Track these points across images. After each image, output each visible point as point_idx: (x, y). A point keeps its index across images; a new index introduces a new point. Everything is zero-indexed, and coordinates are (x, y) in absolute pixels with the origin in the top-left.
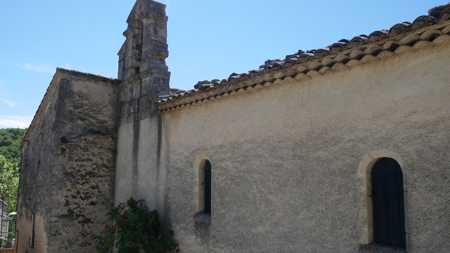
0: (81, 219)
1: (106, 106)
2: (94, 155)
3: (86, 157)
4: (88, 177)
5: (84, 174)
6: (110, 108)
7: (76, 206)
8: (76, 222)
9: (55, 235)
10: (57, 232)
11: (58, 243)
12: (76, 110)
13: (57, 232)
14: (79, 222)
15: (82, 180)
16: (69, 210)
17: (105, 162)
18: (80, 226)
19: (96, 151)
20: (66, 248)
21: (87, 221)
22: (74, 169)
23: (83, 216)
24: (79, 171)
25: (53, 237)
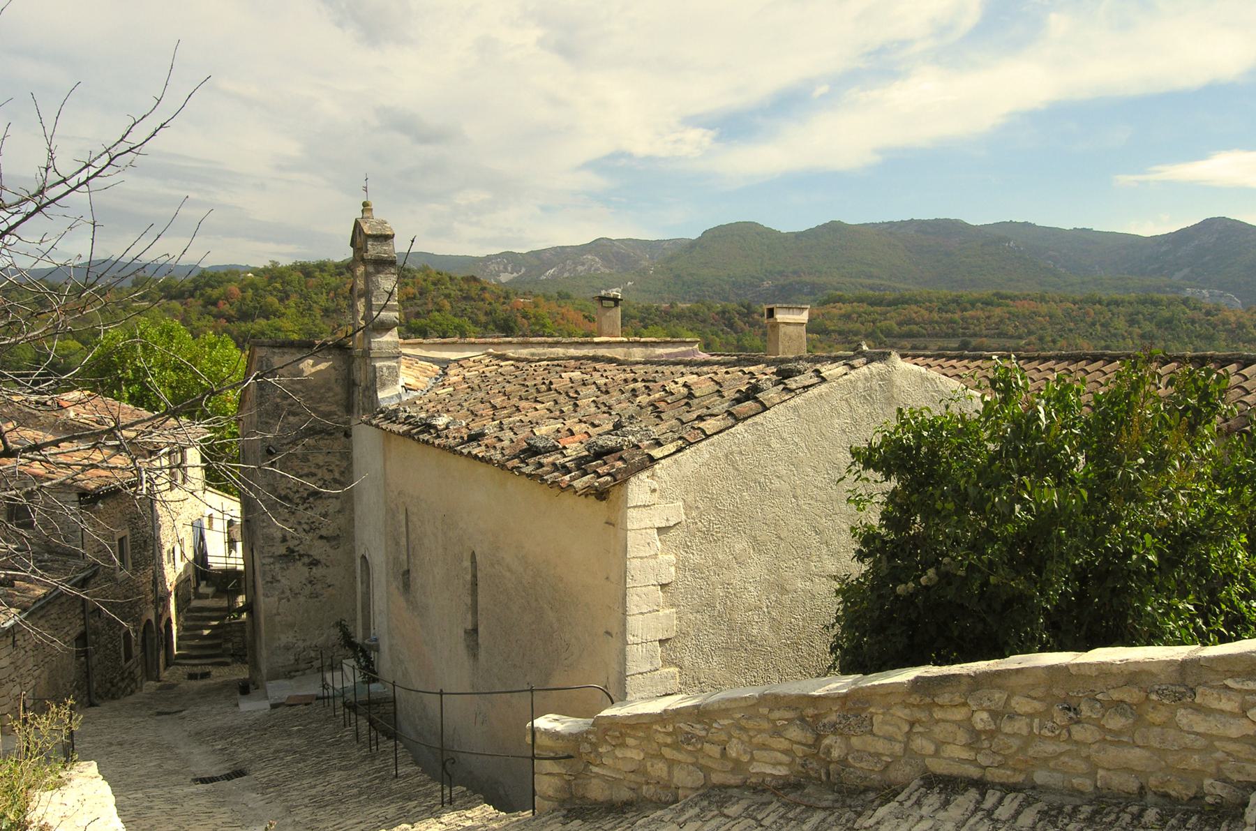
0: (306, 560)
1: (330, 389)
2: (318, 466)
3: (306, 471)
4: (311, 499)
5: (305, 495)
6: (338, 389)
7: (297, 542)
8: (299, 564)
9: (272, 583)
10: (273, 577)
11: (277, 593)
12: (285, 402)
13: (273, 577)
14: (304, 564)
15: (303, 504)
16: (288, 548)
17: (337, 475)
18: (306, 569)
19: (320, 459)
20: (289, 600)
21: (315, 563)
22: (291, 489)
23: (309, 556)
24: (298, 491)
25: (269, 584)
